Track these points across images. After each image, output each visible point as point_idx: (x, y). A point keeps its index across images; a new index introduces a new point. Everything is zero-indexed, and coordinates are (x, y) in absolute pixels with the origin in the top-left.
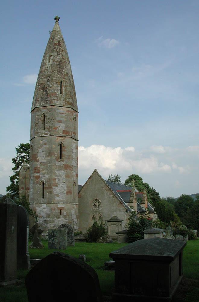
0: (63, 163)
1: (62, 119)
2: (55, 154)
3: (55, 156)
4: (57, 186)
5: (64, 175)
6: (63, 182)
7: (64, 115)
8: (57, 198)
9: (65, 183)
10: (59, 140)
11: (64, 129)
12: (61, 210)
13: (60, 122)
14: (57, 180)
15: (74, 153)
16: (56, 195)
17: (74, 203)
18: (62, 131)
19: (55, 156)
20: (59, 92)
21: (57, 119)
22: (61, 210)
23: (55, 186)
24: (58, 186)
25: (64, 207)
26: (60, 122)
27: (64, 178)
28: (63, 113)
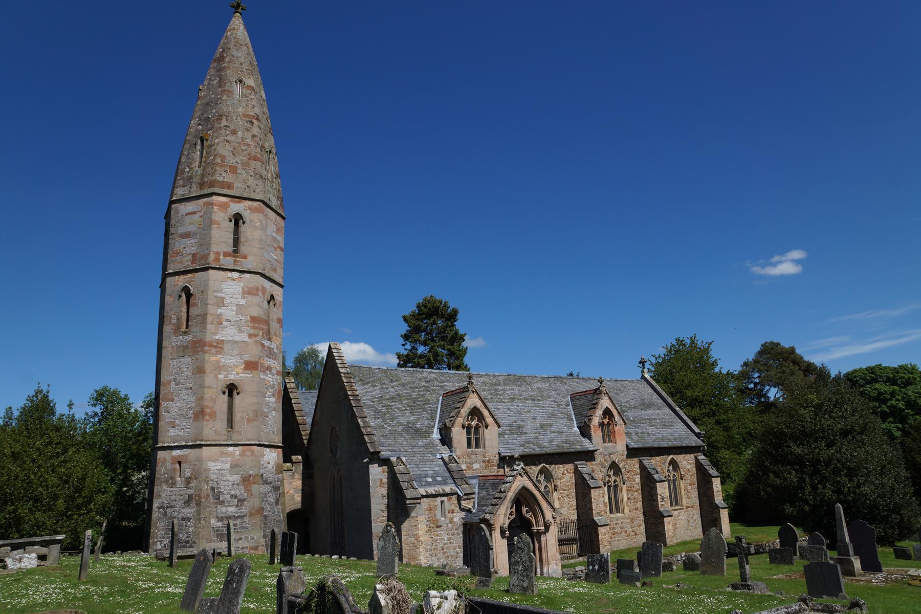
0: (188, 338)
1: (190, 228)
2: (171, 319)
3: (170, 323)
5: (191, 369)
7: (196, 217)
8: (172, 432)
9: (191, 388)
10: (181, 281)
11: (194, 250)
12: (180, 463)
13: (186, 235)
15: (234, 308)
16: (170, 423)
18: (190, 258)
19: (170, 323)
21: (181, 230)
23: (169, 400)
26: (186, 235)
27: (188, 377)
28: (194, 213)
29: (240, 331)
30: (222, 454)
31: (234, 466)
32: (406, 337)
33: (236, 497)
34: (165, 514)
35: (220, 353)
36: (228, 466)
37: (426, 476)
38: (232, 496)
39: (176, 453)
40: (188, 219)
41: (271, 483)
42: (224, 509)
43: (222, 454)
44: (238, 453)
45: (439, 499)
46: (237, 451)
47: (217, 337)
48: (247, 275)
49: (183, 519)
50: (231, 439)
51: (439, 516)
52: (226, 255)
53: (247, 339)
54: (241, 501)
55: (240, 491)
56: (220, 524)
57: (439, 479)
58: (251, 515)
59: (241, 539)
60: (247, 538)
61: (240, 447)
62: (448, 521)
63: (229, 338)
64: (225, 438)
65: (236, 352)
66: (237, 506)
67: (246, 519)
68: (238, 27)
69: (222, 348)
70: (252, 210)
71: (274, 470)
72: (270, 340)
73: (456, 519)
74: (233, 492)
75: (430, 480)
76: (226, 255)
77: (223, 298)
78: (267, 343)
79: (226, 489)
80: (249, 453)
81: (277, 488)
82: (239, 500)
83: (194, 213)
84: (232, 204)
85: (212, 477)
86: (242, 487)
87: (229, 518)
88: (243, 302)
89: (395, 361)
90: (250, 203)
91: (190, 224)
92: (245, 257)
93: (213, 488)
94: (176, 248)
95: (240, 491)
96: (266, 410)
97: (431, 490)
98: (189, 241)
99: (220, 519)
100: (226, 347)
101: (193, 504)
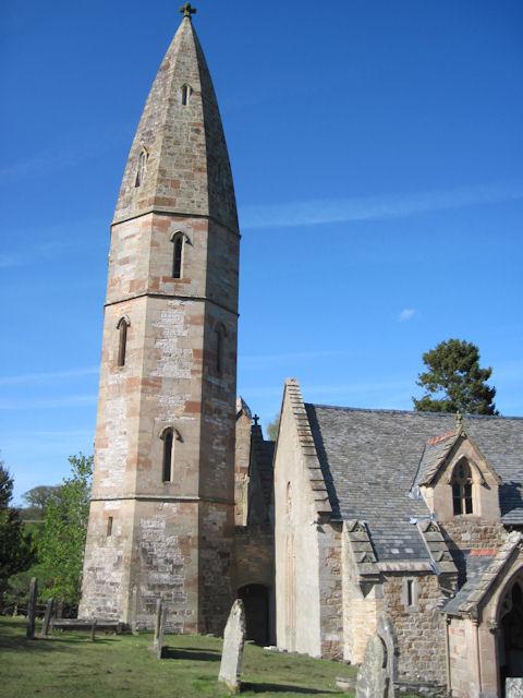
0: (123, 376)
4: (107, 446)
6: (121, 433)
8: (107, 483)
9: (125, 433)
11: (131, 277)
13: (126, 261)
14: (108, 428)
15: (175, 340)
17: (163, 494)
20: (134, 184)
22: (111, 518)
24: (110, 445)
25: (117, 508)
26: (126, 261)
28: (133, 236)
29: (181, 366)
30: (156, 509)
31: (170, 525)
32: (425, 379)
33: (172, 562)
34: (95, 577)
35: (158, 392)
36: (163, 525)
37: (392, 546)
38: (167, 561)
39: (109, 506)
40: (127, 242)
41: (216, 548)
42: (156, 576)
43: (157, 510)
44: (175, 510)
45: (405, 579)
46: (174, 507)
47: (154, 374)
48: (189, 303)
49: (112, 584)
50: (168, 493)
51: (404, 601)
52: (165, 280)
53: (189, 376)
54: (177, 567)
55: (177, 556)
56: (149, 593)
57: (409, 551)
58: (188, 584)
59: (176, 613)
60: (183, 612)
61: (179, 504)
62: (417, 609)
63: (170, 375)
64: (161, 491)
65: (175, 391)
66: (172, 573)
67: (182, 590)
68: (184, 29)
69: (160, 387)
70: (197, 228)
71: (221, 533)
72: (219, 377)
73: (429, 607)
74: (168, 556)
75: (396, 551)
76: (165, 280)
77: (162, 330)
78: (215, 381)
79: (159, 552)
80: (188, 511)
81: (224, 555)
82: (174, 567)
83: (133, 236)
84: (173, 223)
85: (145, 537)
86: (179, 551)
87: (161, 587)
88: (185, 334)
89: (411, 407)
90: (194, 220)
91: (129, 248)
92: (188, 281)
93: (144, 551)
94: (115, 277)
95: (177, 556)
96: (213, 460)
97: (395, 566)
98: (128, 267)
99: (152, 587)
100: (165, 386)
101: (122, 568)
